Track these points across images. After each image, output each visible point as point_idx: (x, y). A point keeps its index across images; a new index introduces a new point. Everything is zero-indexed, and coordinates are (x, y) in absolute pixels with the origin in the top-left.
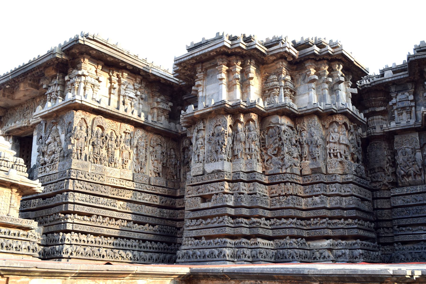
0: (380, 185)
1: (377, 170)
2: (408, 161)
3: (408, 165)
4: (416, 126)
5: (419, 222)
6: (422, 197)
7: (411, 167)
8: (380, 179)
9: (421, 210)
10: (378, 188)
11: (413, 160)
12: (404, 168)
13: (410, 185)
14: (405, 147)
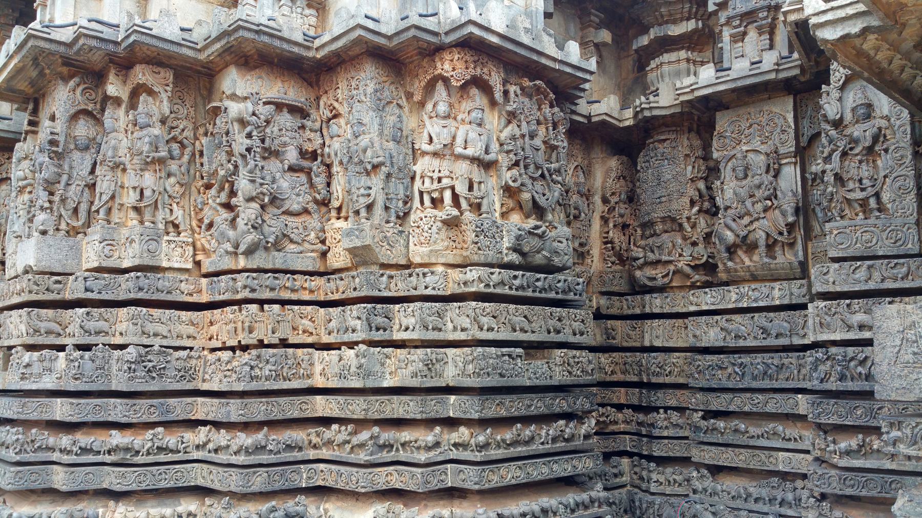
0: (667, 275)
1: (659, 227)
2: (751, 196)
3: (749, 211)
4: (781, 76)
5: (770, 408)
6: (785, 324)
7: (758, 219)
8: (669, 254)
9: (780, 367)
10: (660, 282)
11: (767, 193)
12: (734, 220)
13: (754, 278)
14: (745, 148)
